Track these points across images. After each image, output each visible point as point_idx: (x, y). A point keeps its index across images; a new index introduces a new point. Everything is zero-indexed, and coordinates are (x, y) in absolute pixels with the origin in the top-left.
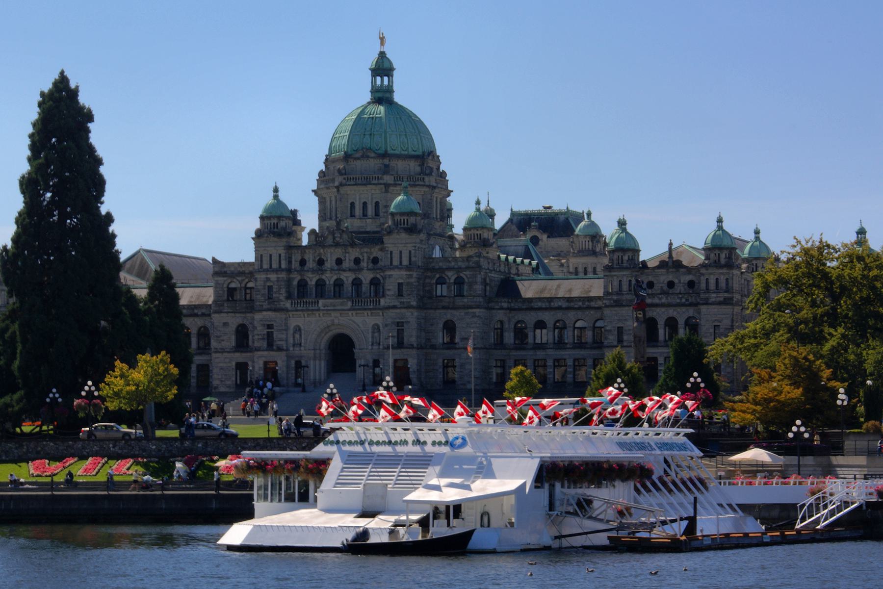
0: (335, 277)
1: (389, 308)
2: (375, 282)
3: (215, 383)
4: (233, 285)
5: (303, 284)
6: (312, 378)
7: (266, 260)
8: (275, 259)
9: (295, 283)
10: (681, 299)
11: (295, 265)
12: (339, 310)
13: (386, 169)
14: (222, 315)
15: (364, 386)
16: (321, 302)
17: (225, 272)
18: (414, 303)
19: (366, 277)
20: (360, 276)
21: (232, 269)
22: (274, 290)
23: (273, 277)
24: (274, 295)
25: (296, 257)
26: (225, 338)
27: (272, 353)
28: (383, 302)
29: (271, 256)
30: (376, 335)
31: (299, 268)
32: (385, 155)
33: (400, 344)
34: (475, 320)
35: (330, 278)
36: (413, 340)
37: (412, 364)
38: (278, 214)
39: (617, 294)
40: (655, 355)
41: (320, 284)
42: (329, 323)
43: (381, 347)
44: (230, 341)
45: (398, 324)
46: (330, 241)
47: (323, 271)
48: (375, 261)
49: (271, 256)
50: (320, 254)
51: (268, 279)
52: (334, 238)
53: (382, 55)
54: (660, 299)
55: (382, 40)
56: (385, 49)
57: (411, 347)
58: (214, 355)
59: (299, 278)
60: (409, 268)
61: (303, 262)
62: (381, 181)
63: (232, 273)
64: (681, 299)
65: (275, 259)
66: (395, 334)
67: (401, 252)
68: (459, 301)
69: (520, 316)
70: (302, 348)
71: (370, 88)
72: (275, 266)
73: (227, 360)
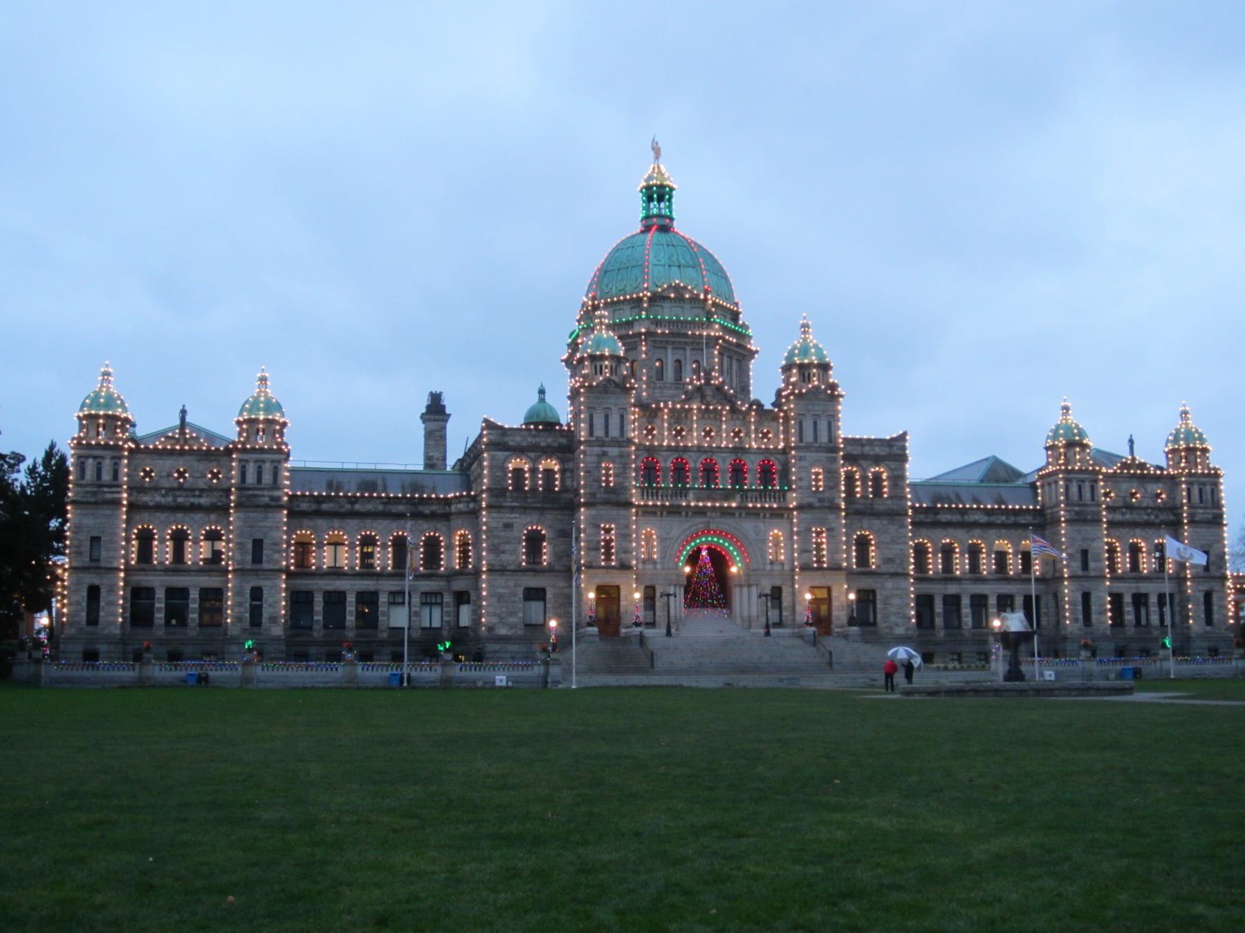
0: (704, 456)
6: (672, 613)
7: (599, 421)
8: (614, 421)
10: (1149, 515)
12: (721, 507)
15: (767, 627)
16: (691, 495)
21: (518, 439)
23: (613, 451)
26: (507, 547)
29: (607, 417)
39: (1079, 505)
40: (1119, 591)
43: (787, 567)
49: (607, 417)
51: (604, 454)
54: (1123, 514)
55: (657, 152)
57: (835, 568)
64: (1149, 515)
65: (614, 421)
67: (815, 423)
70: (659, 566)
71: (642, 214)
73: (511, 584)
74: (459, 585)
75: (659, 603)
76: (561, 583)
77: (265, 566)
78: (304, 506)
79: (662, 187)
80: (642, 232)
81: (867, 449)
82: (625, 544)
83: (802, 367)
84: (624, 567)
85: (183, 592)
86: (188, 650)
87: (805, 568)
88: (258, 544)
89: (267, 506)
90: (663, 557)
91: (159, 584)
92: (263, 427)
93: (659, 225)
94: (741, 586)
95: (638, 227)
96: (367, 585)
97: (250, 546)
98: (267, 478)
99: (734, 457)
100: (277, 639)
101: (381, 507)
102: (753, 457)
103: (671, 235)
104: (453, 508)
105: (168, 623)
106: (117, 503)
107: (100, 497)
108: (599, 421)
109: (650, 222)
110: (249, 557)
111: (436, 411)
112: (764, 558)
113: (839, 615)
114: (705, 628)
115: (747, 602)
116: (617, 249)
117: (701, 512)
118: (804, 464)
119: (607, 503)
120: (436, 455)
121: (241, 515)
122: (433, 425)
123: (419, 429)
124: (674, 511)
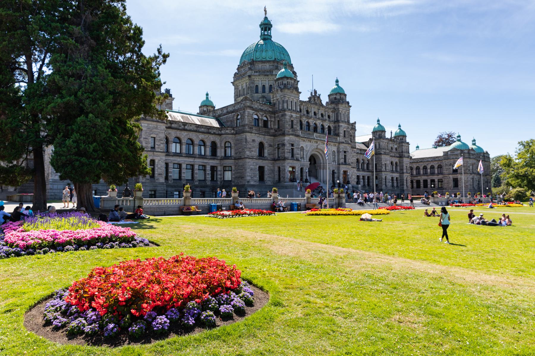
8: (294, 104)
14: (253, 134)
17: (252, 107)
21: (256, 106)
23: (294, 115)
24: (295, 126)
26: (254, 149)
27: (295, 162)
33: (345, 163)
44: (256, 153)
45: (345, 152)
50: (308, 107)
51: (292, 116)
52: (314, 100)
58: (248, 160)
63: (256, 108)
65: (294, 104)
73: (255, 164)
82: (298, 152)
87: (342, 164)
94: (323, 169)
99: (322, 123)
101: (195, 129)
104: (223, 132)
119: (292, 135)
124: (310, 140)
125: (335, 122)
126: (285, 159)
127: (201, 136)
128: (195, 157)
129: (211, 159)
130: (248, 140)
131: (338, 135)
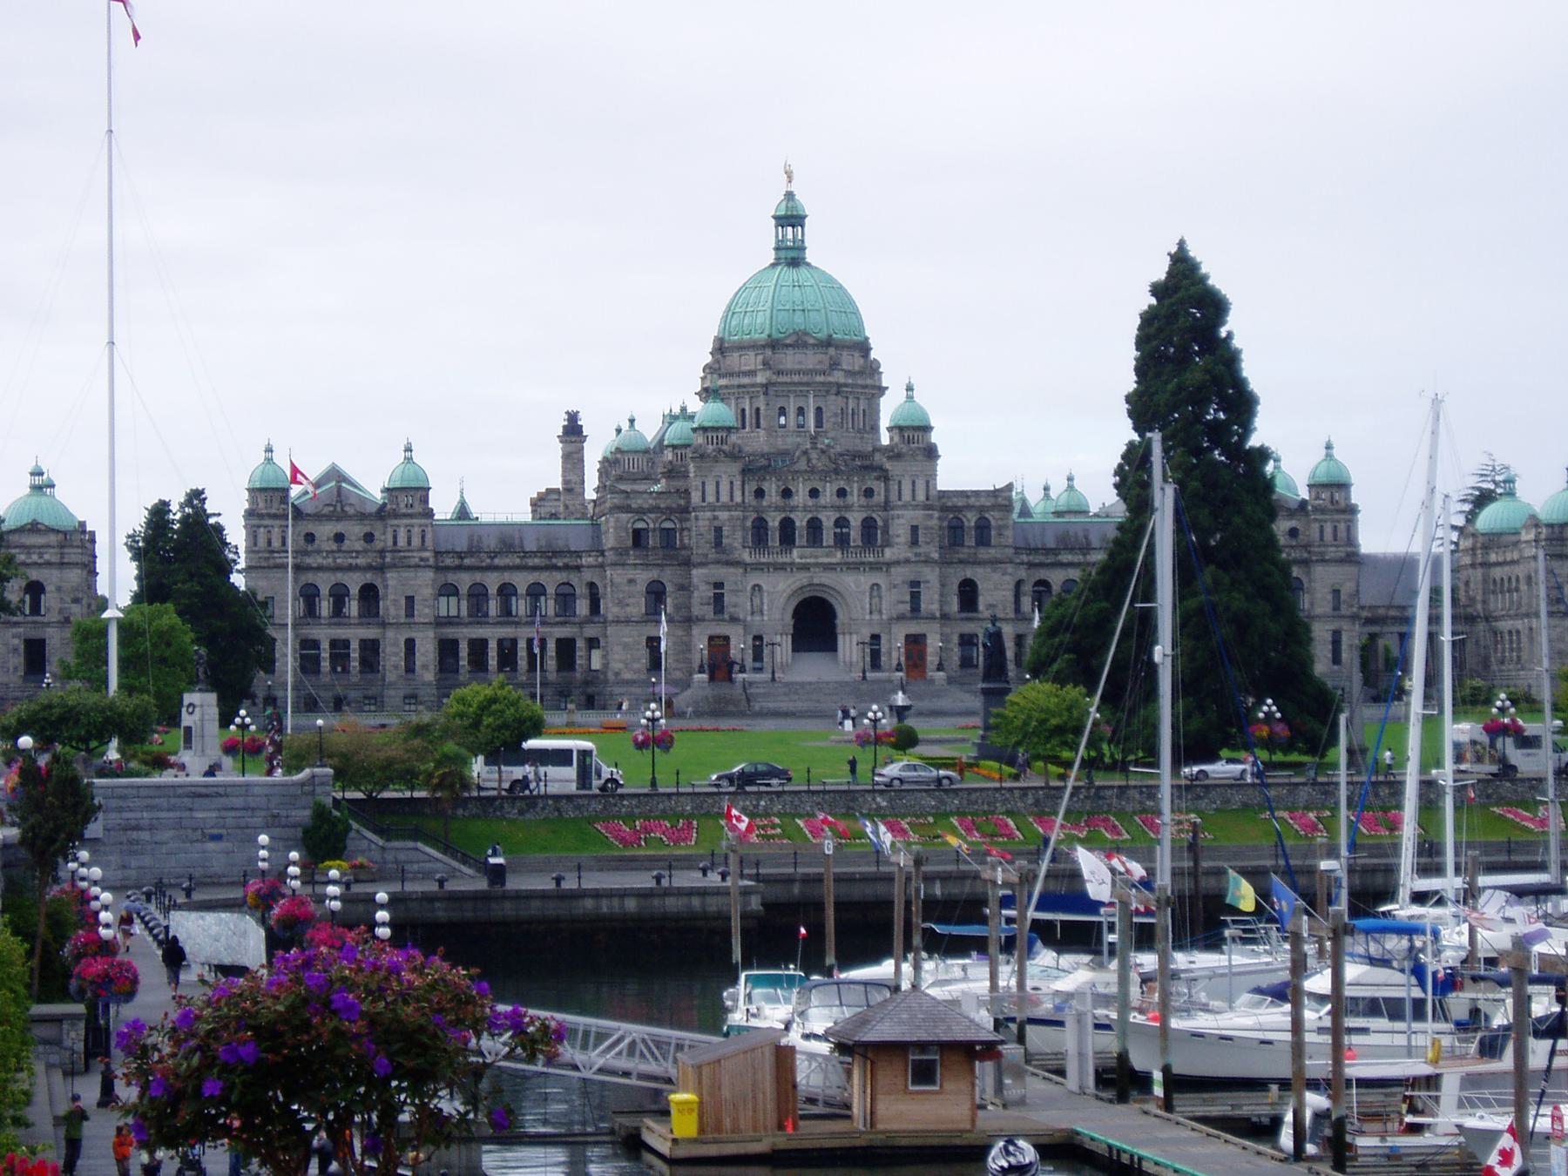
1: (898, 563)
2: (869, 526)
3: (616, 666)
4: (640, 525)
5: (760, 527)
7: (710, 489)
8: (724, 488)
9: (749, 524)
11: (750, 499)
13: (834, 365)
15: (864, 672)
16: (795, 551)
18: (936, 556)
19: (855, 519)
20: (847, 515)
22: (725, 533)
23: (723, 515)
25: (751, 487)
26: (631, 601)
28: (888, 552)
30: (876, 600)
31: (754, 503)
32: (828, 343)
34: (1007, 578)
35: (800, 521)
36: (935, 607)
37: (934, 643)
38: (728, 424)
41: (787, 527)
42: (805, 582)
44: (638, 607)
45: (915, 584)
46: (802, 465)
47: (793, 509)
48: (869, 493)
51: (715, 518)
52: (809, 460)
53: (790, 196)
56: (793, 188)
57: (933, 618)
59: (754, 515)
60: (927, 507)
61: (760, 493)
62: (831, 379)
65: (724, 488)
66: (908, 598)
68: (984, 553)
69: (1043, 574)
72: (725, 498)
74: (590, 631)
75: (766, 651)
76: (680, 633)
77: (416, 619)
78: (448, 561)
79: (792, 216)
80: (773, 265)
81: (972, 500)
83: (901, 429)
84: (734, 620)
85: (346, 644)
86: (353, 694)
87: (901, 618)
88: (410, 600)
89: (418, 566)
90: (770, 609)
91: (324, 634)
92: (409, 497)
93: (791, 257)
95: (771, 257)
96: (507, 632)
97: (403, 602)
98: (416, 541)
100: (429, 684)
101: (518, 561)
102: (856, 515)
103: (803, 270)
105: (334, 669)
106: (284, 566)
107: (271, 562)
108: (710, 489)
109: (783, 254)
110: (403, 613)
111: (573, 431)
112: (863, 608)
113: (932, 659)
114: (812, 669)
115: (850, 647)
116: (744, 288)
117: (805, 567)
118: (902, 521)
119: (718, 562)
120: (574, 478)
121: (395, 575)
122: (571, 448)
123: (557, 450)
124: (780, 567)
125: (887, 506)
126: (701, 620)
127: (532, 577)
128: (517, 624)
129: (557, 624)
130: (617, 579)
131: (887, 543)
